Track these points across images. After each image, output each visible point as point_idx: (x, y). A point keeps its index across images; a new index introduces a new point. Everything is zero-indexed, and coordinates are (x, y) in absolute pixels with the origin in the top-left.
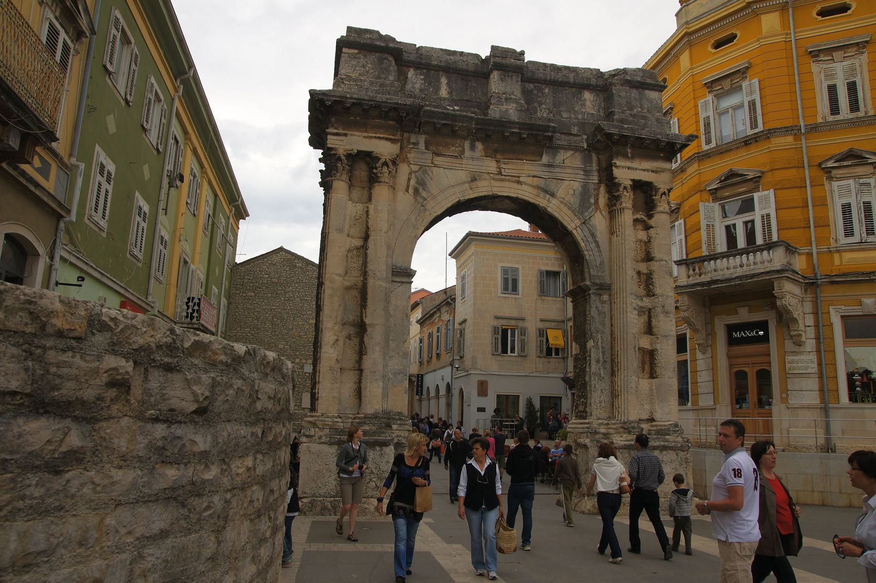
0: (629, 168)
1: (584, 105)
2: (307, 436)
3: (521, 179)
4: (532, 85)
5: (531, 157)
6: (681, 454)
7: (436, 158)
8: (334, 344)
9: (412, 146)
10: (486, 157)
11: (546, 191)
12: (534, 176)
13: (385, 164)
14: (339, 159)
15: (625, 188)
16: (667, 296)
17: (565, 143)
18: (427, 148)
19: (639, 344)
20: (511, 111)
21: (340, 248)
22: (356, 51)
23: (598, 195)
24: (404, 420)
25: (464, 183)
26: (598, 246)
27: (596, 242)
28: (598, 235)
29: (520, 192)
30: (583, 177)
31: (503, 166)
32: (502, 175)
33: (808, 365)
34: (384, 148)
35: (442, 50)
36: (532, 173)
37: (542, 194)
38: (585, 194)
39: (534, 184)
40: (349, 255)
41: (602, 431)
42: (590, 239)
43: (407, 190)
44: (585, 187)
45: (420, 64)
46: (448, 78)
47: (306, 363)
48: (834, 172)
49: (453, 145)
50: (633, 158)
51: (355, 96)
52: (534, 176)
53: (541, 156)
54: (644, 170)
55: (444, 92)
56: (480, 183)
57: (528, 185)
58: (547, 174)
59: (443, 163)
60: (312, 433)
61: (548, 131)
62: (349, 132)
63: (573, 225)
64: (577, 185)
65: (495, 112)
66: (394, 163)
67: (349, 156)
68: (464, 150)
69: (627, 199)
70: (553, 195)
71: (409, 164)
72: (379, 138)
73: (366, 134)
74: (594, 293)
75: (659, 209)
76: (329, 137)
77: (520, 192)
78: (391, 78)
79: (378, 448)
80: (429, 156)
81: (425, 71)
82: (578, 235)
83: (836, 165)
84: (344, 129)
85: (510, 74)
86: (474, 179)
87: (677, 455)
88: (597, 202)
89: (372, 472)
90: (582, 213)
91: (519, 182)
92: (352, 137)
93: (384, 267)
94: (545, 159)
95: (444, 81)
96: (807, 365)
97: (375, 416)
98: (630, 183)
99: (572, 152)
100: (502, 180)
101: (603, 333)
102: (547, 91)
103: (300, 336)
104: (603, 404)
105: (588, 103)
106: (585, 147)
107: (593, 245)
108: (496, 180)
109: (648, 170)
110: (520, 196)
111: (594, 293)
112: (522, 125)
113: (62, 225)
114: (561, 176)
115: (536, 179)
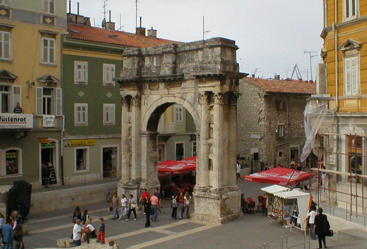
0: (203, 87)
4: (181, 54)
5: (178, 85)
6: (216, 201)
7: (152, 91)
8: (124, 158)
9: (145, 88)
10: (165, 88)
12: (179, 93)
13: (134, 98)
15: (202, 95)
16: (215, 139)
17: (187, 78)
18: (149, 88)
19: (208, 157)
20: (167, 71)
21: (124, 128)
22: (127, 58)
24: (144, 181)
25: (159, 99)
30: (194, 91)
31: (169, 91)
32: (169, 94)
34: (133, 93)
36: (178, 92)
39: (179, 96)
42: (197, 116)
43: (144, 105)
46: (156, 57)
47: (251, 134)
48: (346, 52)
49: (156, 85)
52: (179, 93)
53: (181, 84)
54: (209, 87)
55: (155, 64)
59: (154, 93)
62: (124, 89)
63: (191, 112)
64: (193, 95)
65: (162, 73)
66: (137, 97)
67: (125, 97)
68: (159, 86)
69: (204, 100)
76: (121, 92)
78: (136, 65)
79: (133, 190)
80: (149, 91)
81: (149, 57)
83: (344, 49)
86: (161, 98)
87: (215, 201)
91: (175, 97)
93: (134, 134)
94: (183, 85)
98: (205, 93)
100: (170, 96)
102: (186, 55)
103: (248, 120)
108: (168, 97)
109: (210, 87)
111: (197, 137)
112: (169, 76)
113: (62, 133)
114: (187, 92)
115: (180, 94)
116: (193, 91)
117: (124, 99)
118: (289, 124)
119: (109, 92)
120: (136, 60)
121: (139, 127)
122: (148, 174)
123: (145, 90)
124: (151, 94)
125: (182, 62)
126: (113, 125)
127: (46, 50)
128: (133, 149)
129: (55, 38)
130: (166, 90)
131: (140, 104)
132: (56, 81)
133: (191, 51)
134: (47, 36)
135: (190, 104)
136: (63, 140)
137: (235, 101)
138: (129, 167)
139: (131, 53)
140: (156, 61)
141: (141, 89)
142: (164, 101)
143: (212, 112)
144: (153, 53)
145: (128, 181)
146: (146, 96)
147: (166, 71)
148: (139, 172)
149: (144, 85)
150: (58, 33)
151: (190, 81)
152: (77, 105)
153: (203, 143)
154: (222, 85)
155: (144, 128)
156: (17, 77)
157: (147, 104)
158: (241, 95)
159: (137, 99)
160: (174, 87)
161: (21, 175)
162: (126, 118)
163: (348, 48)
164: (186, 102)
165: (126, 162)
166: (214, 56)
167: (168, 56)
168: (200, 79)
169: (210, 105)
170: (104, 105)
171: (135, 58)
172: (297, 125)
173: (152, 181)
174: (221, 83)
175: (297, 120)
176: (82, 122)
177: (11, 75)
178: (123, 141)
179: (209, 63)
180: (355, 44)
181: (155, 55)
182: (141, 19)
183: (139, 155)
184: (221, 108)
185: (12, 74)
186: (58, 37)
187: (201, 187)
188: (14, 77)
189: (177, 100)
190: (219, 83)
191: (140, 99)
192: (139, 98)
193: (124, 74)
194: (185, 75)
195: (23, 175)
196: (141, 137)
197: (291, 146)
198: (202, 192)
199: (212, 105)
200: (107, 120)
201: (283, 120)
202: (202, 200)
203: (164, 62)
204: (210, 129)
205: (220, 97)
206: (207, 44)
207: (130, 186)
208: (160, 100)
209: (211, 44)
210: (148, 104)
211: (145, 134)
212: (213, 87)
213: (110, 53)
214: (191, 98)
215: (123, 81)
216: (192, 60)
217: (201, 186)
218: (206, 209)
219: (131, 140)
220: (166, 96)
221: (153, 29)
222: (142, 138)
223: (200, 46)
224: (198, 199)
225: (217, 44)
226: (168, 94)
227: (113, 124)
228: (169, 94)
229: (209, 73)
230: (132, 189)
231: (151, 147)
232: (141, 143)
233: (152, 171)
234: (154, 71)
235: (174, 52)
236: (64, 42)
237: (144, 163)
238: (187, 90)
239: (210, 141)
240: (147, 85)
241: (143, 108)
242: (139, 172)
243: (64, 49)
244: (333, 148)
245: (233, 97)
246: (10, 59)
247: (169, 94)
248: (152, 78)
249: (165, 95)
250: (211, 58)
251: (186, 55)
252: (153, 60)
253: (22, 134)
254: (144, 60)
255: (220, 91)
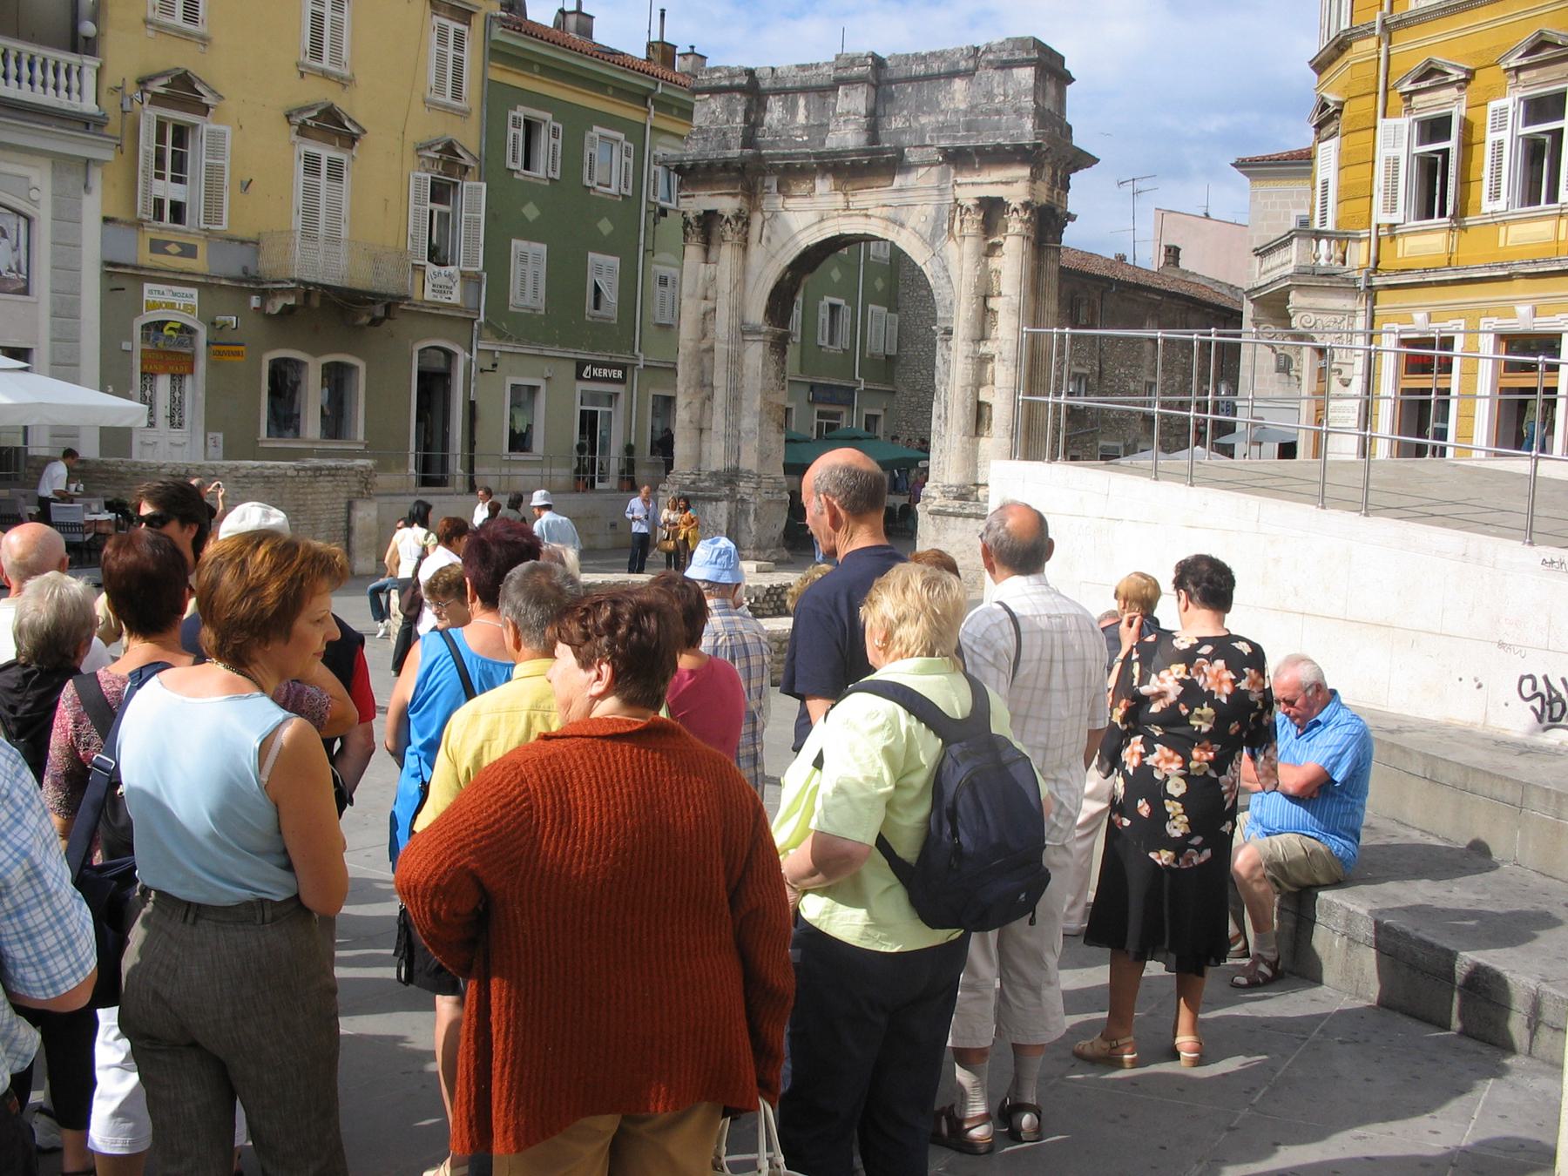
0: (973, 184)
1: (954, 99)
2: (664, 491)
3: (869, 213)
10: (836, 190)
11: (894, 222)
12: (884, 206)
13: (728, 220)
14: (689, 222)
15: (968, 210)
20: (849, 136)
22: (707, 96)
23: (954, 219)
25: (813, 224)
26: (950, 281)
27: (949, 277)
28: (950, 268)
29: (868, 227)
30: (937, 198)
31: (851, 199)
33: (1349, 415)
34: (727, 204)
35: (797, 66)
36: (881, 202)
37: (891, 226)
38: (937, 220)
40: (708, 318)
41: (933, 494)
42: (941, 274)
43: (760, 242)
44: (939, 208)
45: (775, 89)
48: (1415, 99)
50: (980, 170)
51: (691, 158)
52: (884, 206)
54: (992, 183)
55: (801, 118)
56: (826, 224)
57: (876, 217)
58: (896, 200)
60: (666, 488)
61: (884, 154)
62: (696, 193)
64: (930, 210)
65: (832, 142)
66: (738, 217)
67: (698, 218)
69: (972, 224)
70: (902, 225)
71: (762, 212)
72: (721, 194)
73: (709, 193)
74: (941, 339)
75: (1010, 230)
77: (868, 227)
78: (738, 120)
79: (714, 503)
82: (927, 270)
83: (1412, 88)
84: (693, 189)
85: (855, 85)
86: (822, 220)
88: (951, 227)
89: (709, 525)
90: (932, 244)
91: (866, 216)
92: (701, 198)
94: (898, 181)
95: (802, 102)
96: (1349, 415)
97: (715, 474)
99: (927, 168)
100: (851, 216)
101: (947, 384)
102: (910, 89)
104: (941, 465)
105: (958, 96)
106: (941, 159)
107: (943, 282)
108: (845, 216)
110: (868, 232)
111: (941, 339)
112: (857, 152)
113: (476, 325)
114: (909, 201)
115: (885, 208)
116: (932, 198)
117: (695, 224)
118: (1100, 372)
119: (606, 219)
120: (740, 103)
121: (739, 309)
122: (764, 457)
123: (763, 199)
124: (787, 210)
125: (896, 111)
126: (612, 322)
127: (441, 57)
128: (720, 379)
129: (469, 24)
130: (840, 197)
131: (746, 240)
132: (467, 160)
133: (928, 77)
134: (446, 15)
135: (922, 237)
136: (478, 350)
137: (1058, 237)
138: (698, 432)
139: (726, 83)
140: (806, 106)
141: (752, 193)
142: (830, 230)
143: (994, 263)
144: (798, 84)
145: (693, 477)
146: (768, 215)
147: (846, 136)
148: (735, 450)
149: (763, 182)
150: (479, 8)
151: (922, 171)
152: (518, 245)
153: (965, 354)
154: (1034, 178)
155: (756, 313)
156: (364, 132)
157: (769, 239)
158: (1072, 218)
159: (740, 224)
160: (867, 188)
161: (360, 443)
162: (697, 283)
163: (1423, 85)
164: (905, 233)
165: (691, 417)
166: (1011, 92)
167: (853, 92)
168: (958, 158)
169: (990, 241)
170: (591, 255)
171: (738, 96)
172: (1120, 380)
173: (772, 481)
174: (1031, 174)
175: (1122, 365)
176: (528, 301)
177: (347, 124)
178: (684, 354)
179: (998, 112)
180: (1449, 70)
181: (805, 90)
182: (663, 15)
183: (735, 399)
184: (1027, 246)
185: (350, 120)
186: (478, 22)
187: (951, 486)
188: (355, 130)
189: (874, 228)
190: (1025, 172)
191: (747, 224)
192: (743, 220)
193: (697, 144)
194: (906, 150)
195: (366, 446)
196: (744, 340)
197: (1101, 443)
198: (955, 498)
199: (996, 240)
200: (597, 307)
201: (1085, 358)
202: (952, 526)
203: (838, 110)
204: (985, 315)
205: (1026, 217)
206: (991, 57)
207: (702, 490)
208: (815, 228)
209: (1005, 56)
210: (772, 240)
211: (759, 333)
212: (1007, 183)
213: (612, 96)
214: (923, 219)
215: (695, 166)
216: (933, 107)
217: (951, 483)
218: (967, 548)
219: (711, 349)
220: (839, 216)
221: (696, 51)
222: (748, 344)
223: (963, 65)
224: (942, 520)
225: (1025, 56)
226: (844, 210)
227: (609, 319)
228: (848, 208)
229: (1000, 140)
230: (711, 499)
231: (772, 374)
232: (743, 360)
233: (771, 450)
234: (800, 140)
235: (875, 82)
236: (496, 42)
237: (749, 422)
238: (909, 197)
239: (985, 349)
240: (772, 182)
241: (755, 250)
242: (735, 450)
243: (492, 63)
244: (1350, 380)
245: (1053, 223)
246: (346, 73)
247: (848, 208)
248: (794, 159)
249: (836, 213)
250: (1002, 98)
251: (910, 89)
252: (795, 105)
253: (379, 311)
254: (763, 108)
255: (1028, 198)
